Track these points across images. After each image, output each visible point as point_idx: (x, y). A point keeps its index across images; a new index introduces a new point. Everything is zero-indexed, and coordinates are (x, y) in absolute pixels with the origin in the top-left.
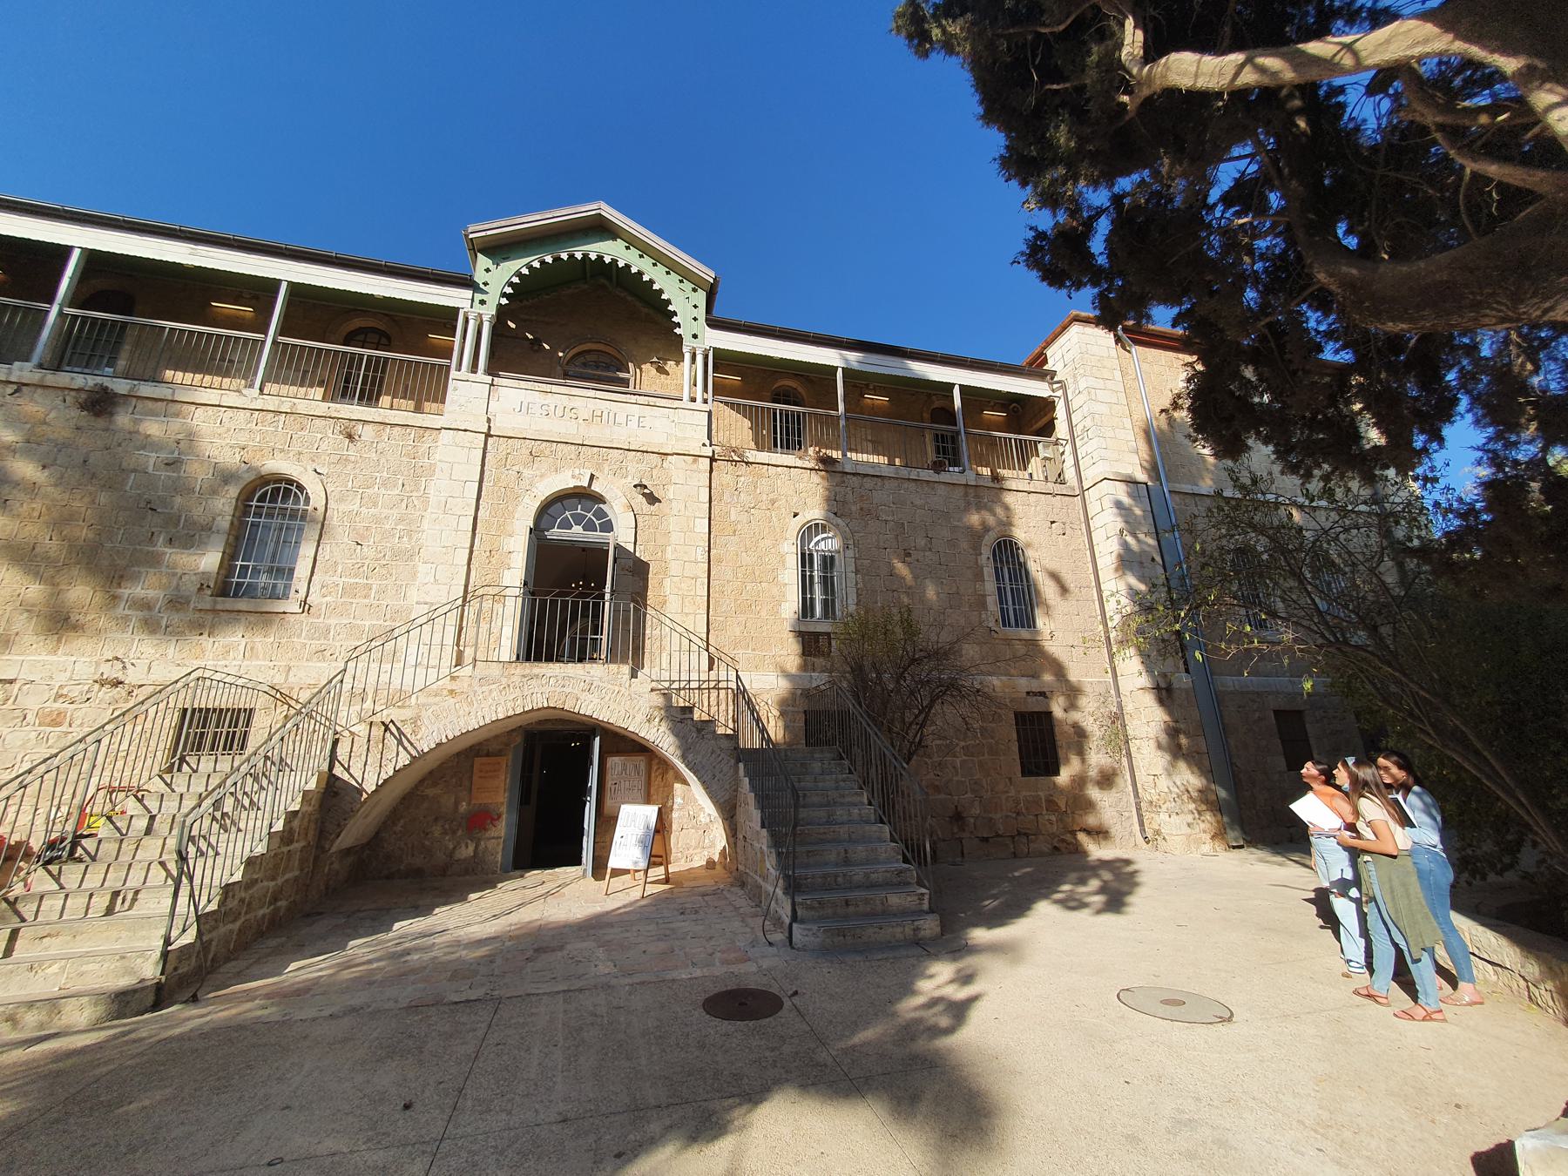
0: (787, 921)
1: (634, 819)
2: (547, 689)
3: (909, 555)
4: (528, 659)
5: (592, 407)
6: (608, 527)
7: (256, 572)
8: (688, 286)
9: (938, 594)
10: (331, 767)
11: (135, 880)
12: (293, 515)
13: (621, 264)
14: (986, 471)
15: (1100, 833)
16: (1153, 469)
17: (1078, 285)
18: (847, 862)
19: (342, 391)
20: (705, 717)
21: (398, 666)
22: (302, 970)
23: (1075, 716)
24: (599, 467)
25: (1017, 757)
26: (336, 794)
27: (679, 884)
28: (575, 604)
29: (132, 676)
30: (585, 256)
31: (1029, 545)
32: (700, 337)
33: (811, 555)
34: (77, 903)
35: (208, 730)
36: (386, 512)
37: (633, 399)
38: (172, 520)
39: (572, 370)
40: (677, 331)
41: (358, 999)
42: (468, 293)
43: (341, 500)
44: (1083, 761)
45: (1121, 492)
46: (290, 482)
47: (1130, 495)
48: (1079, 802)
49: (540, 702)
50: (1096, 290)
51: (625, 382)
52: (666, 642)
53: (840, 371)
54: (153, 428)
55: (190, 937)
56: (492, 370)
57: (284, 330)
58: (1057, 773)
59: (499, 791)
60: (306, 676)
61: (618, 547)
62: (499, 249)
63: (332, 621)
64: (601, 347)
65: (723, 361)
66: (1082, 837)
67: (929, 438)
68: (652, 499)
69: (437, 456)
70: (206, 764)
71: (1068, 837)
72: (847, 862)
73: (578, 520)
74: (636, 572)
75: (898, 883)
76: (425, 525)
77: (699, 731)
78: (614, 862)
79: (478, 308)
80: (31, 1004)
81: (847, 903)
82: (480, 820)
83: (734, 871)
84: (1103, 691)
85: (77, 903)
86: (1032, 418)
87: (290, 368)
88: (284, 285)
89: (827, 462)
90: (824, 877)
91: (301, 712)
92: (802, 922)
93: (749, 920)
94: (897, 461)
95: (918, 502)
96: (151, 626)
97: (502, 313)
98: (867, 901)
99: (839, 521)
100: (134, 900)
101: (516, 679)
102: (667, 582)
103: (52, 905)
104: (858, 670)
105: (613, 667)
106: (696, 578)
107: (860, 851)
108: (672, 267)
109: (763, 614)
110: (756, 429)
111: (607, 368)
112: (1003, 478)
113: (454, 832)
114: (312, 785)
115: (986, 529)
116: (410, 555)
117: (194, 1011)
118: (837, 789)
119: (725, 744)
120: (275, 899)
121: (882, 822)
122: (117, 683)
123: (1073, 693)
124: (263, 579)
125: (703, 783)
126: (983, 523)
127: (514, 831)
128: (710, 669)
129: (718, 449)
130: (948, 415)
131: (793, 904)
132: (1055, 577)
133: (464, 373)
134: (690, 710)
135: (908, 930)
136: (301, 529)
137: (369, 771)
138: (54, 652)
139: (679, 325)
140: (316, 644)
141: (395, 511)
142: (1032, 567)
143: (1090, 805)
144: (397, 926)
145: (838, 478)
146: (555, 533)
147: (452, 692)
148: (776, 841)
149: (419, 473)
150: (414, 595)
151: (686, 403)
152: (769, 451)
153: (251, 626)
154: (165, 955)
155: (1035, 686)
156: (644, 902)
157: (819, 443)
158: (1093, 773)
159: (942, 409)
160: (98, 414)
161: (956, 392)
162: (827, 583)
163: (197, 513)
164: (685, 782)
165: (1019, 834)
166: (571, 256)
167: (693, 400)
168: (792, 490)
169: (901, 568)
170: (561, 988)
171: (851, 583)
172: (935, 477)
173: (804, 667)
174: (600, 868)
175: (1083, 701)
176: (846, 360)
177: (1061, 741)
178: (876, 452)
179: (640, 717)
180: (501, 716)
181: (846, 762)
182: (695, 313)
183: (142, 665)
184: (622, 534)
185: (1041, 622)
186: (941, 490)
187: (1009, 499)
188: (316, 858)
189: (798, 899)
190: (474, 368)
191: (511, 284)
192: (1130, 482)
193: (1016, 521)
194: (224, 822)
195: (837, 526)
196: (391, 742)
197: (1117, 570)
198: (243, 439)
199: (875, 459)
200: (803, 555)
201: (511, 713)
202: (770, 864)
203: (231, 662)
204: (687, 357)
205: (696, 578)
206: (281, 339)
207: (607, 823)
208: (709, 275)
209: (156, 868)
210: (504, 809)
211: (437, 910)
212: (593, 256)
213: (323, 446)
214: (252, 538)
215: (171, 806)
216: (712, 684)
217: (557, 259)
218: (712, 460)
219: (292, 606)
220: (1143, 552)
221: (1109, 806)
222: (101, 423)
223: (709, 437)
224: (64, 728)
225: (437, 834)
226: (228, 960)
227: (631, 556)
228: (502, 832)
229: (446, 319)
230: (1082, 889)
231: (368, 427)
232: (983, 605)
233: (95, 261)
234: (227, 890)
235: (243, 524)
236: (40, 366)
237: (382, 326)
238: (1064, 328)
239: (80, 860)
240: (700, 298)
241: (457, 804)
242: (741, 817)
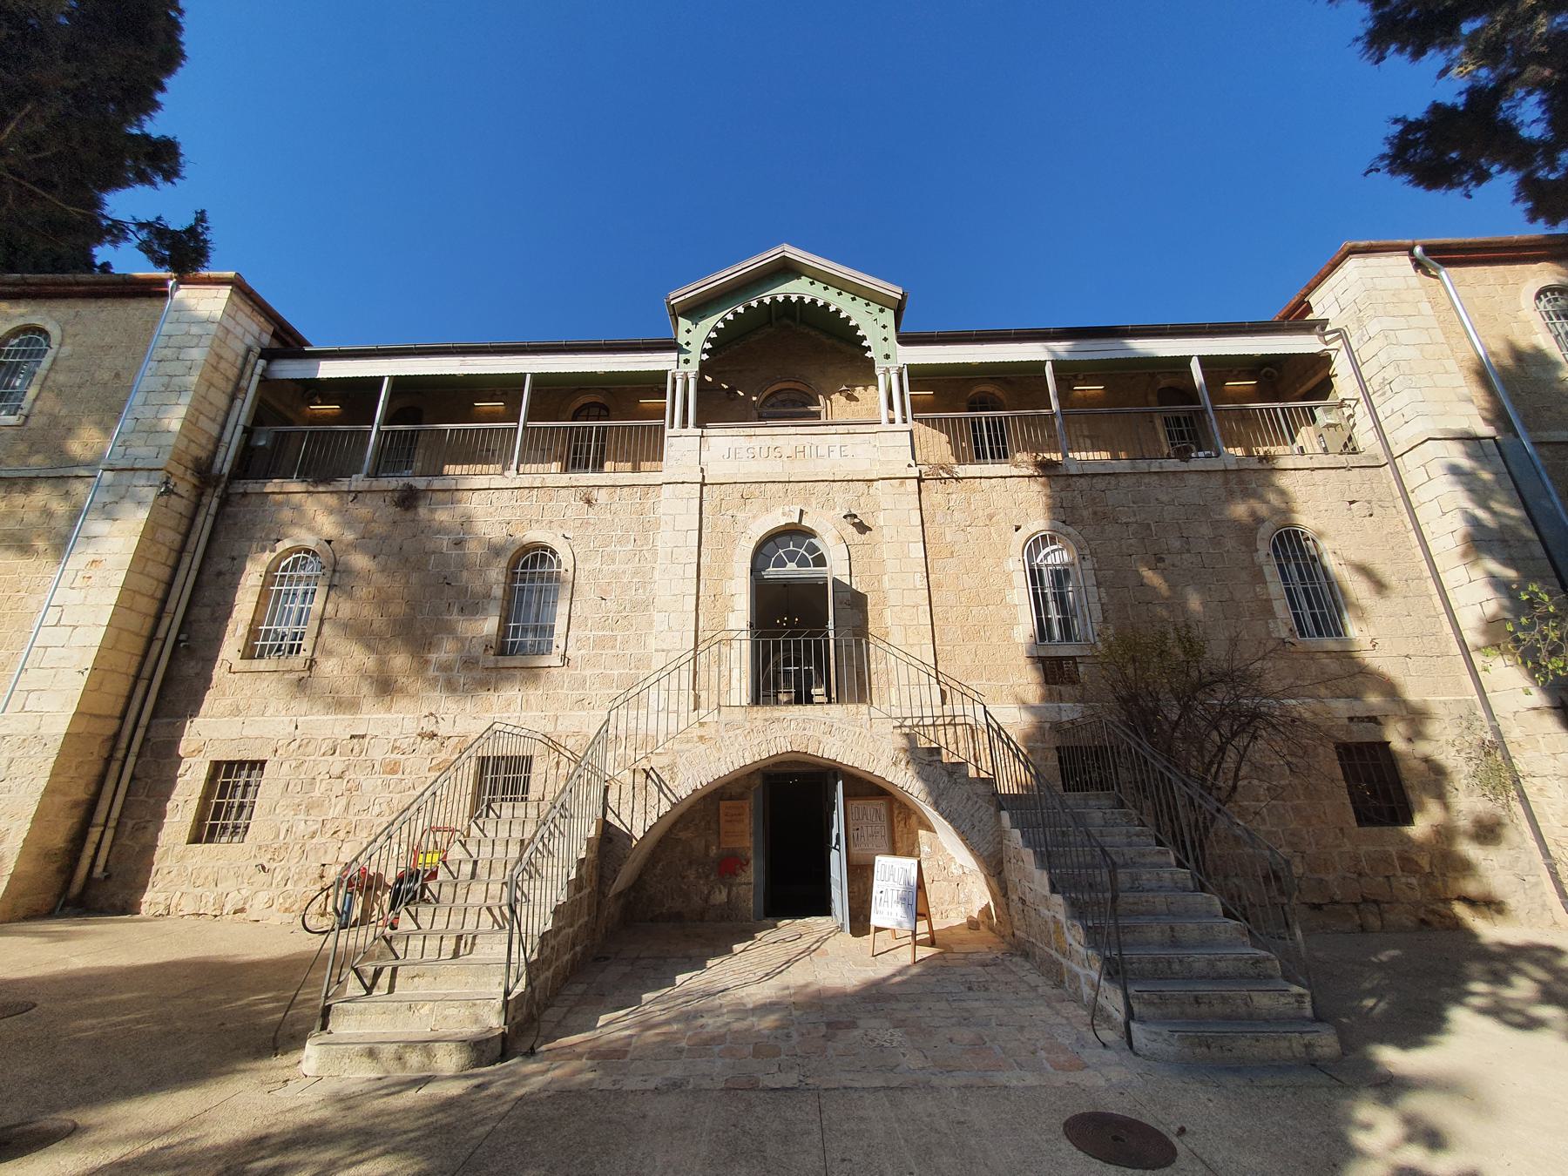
0: (1120, 1017)
1: (892, 875)
2: (789, 733)
3: (1161, 560)
4: (757, 703)
5: (794, 444)
6: (820, 561)
7: (525, 631)
8: (875, 308)
9: (1204, 604)
10: (604, 815)
11: (470, 926)
12: (549, 579)
13: (807, 300)
14: (1239, 452)
15: (1491, 905)
16: (1498, 417)
17: (1482, 177)
18: (1175, 943)
19: (576, 460)
20: (955, 759)
21: (643, 712)
22: (614, 1025)
23: (1423, 748)
24: (807, 501)
25: (1348, 802)
26: (610, 840)
27: (947, 949)
28: (807, 644)
29: (443, 730)
30: (774, 299)
31: (1320, 535)
32: (892, 356)
33: (1040, 571)
34: (432, 944)
35: (501, 778)
36: (623, 567)
37: (833, 429)
38: (463, 591)
39: (766, 410)
40: (868, 354)
41: (676, 1072)
42: (673, 356)
43: (586, 560)
44: (1446, 807)
45: (1456, 454)
46: (545, 548)
47: (1470, 456)
48: (1444, 862)
50: (1521, 174)
51: (817, 415)
52: (893, 676)
53: (1049, 369)
54: (443, 516)
55: (520, 988)
56: (700, 424)
57: (530, 417)
58: (1409, 821)
59: (745, 834)
60: (577, 725)
61: (835, 581)
62: (696, 310)
63: (588, 672)
64: (791, 385)
65: (919, 376)
66: (1460, 910)
67: (1159, 423)
68: (862, 528)
70: (507, 811)
71: (1440, 907)
72: (1175, 943)
73: (792, 556)
74: (856, 603)
75: (1257, 976)
76: (657, 576)
77: (950, 774)
78: (875, 920)
79: (684, 368)
80: (411, 1044)
81: (1197, 1000)
82: (729, 865)
83: (1008, 939)
84: (1465, 713)
85: (432, 944)
86: (1304, 380)
87: (537, 450)
89: (1046, 468)
90: (1155, 962)
91: (584, 763)
92: (1142, 1021)
93: (1058, 1006)
94: (1123, 455)
95: (1165, 498)
96: (451, 687)
97: (704, 367)
98: (1224, 1000)
99: (1070, 529)
100: (473, 944)
101: (759, 723)
102: (887, 613)
103: (416, 943)
104: (1129, 701)
105: (852, 707)
106: (916, 606)
107: (1190, 930)
108: (857, 292)
109: (994, 640)
110: (954, 442)
111: (794, 403)
112: (1274, 457)
113: (707, 877)
114: (592, 833)
115: (1258, 520)
116: (645, 605)
117: (532, 1067)
118: (1130, 845)
119: (981, 789)
120: (574, 945)
121: (1203, 889)
122: (433, 736)
123: (1417, 719)
124: (530, 638)
125: (956, 828)
126: (1253, 514)
127: (762, 877)
128: (943, 703)
129: (925, 469)
130: (1188, 394)
131: (1126, 997)
132: (1364, 570)
133: (677, 429)
134: (938, 750)
135: (1298, 1048)
136: (556, 590)
137: (638, 818)
138: (389, 710)
139: (869, 349)
140: (576, 695)
141: (630, 565)
142: (1330, 561)
143: (1466, 867)
144: (679, 979)
145: (1062, 482)
146: (771, 572)
147: (701, 738)
148: (1078, 910)
149: (647, 527)
150: (653, 644)
151: (885, 425)
152: (972, 463)
153: (525, 681)
154: (506, 1003)
155: (1359, 710)
156: (915, 970)
157: (1036, 448)
158: (1464, 823)
159: (1171, 388)
160: (407, 509)
161: (1195, 368)
162: (1061, 600)
163: (477, 585)
164: (930, 829)
165: (1365, 900)
166: (761, 302)
167: (892, 421)
168: (1008, 504)
169: (1151, 577)
170: (878, 1083)
171: (1094, 599)
172: (1183, 466)
173: (1048, 697)
174: (860, 922)
175: (1433, 728)
176: (1053, 352)
177: (1409, 779)
178: (1095, 448)
179: (885, 761)
180: (748, 762)
181: (1134, 812)
182: (885, 333)
183: (449, 718)
184: (836, 568)
185: (1353, 629)
186: (1193, 480)
187: (1284, 481)
188: (599, 903)
189: (1131, 991)
190: (685, 424)
191: (709, 340)
192: (1467, 438)
193: (1298, 505)
194: (532, 871)
195: (1068, 535)
196: (653, 788)
197: (1465, 555)
198: (507, 515)
199: (1097, 456)
200: (1032, 571)
201: (757, 758)
202: (1074, 937)
203: (508, 714)
204: (881, 379)
205: (916, 606)
206: (530, 424)
207: (861, 875)
208: (895, 292)
209: (484, 912)
210: (751, 854)
211: (709, 963)
212: (780, 298)
213: (569, 513)
214: (520, 602)
215: (486, 850)
216: (947, 720)
217: (748, 308)
218: (920, 480)
219: (554, 660)
220: (1503, 527)
221: (1493, 868)
222: (409, 515)
223: (914, 458)
224: (399, 776)
225: (692, 878)
226: (547, 1007)
227: (848, 588)
228: (751, 880)
229: (655, 383)
230: (1508, 993)
231: (603, 491)
232: (1267, 610)
233: (401, 384)
234: (544, 937)
235: (512, 590)
236: (368, 476)
237: (600, 400)
238: (1335, 266)
239: (428, 902)
240: (889, 315)
241: (707, 847)
242: (1012, 876)
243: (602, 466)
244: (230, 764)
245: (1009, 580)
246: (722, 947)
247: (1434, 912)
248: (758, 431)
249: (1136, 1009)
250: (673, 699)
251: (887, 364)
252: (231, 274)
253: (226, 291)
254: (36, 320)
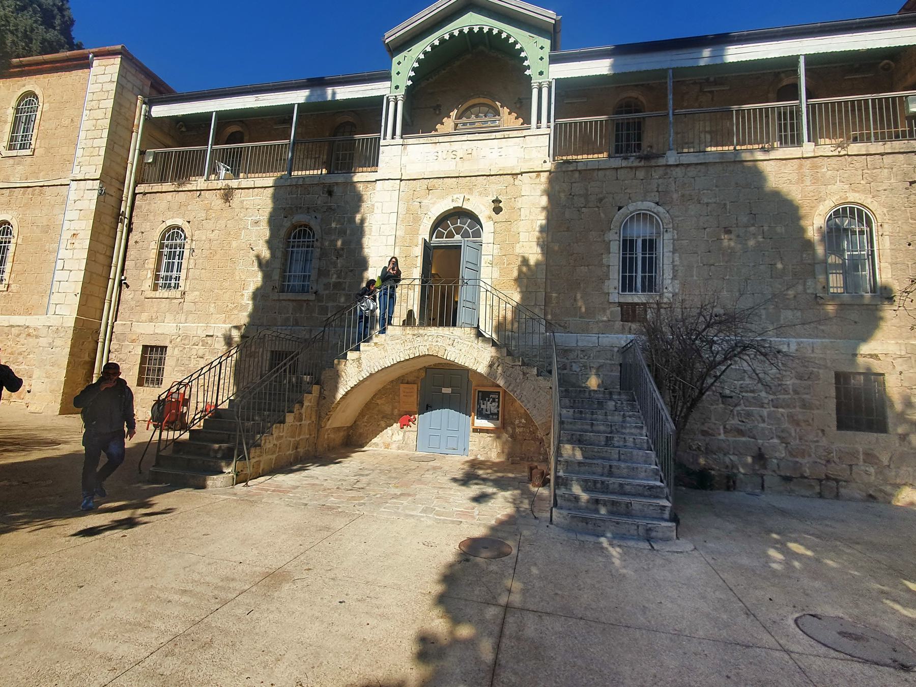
25: (834, 416)
28: (443, 288)
40: (527, 72)
49: (423, 351)
63: (330, 304)
69: (374, 200)
72: (611, 474)
88: (296, 106)
92: (561, 508)
165: (828, 478)
182: (541, 53)
201: (407, 358)
222: (228, 204)
243: (238, 175)
244: (152, 347)
247: (881, 491)
248: (422, 140)
249: (559, 501)
251: (541, 79)
252: (119, 47)
253: (117, 60)
254: (28, 88)
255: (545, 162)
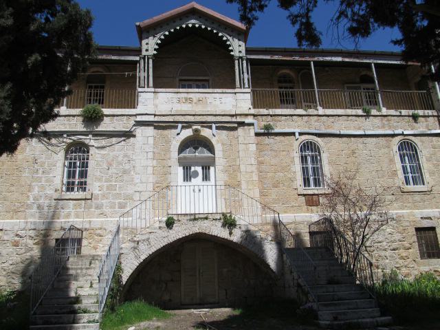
30: (187, 26)
180: (181, 237)
232: (395, 173)
245: (293, 161)
246: (169, 310)
250: (143, 213)
255: (250, 109)
